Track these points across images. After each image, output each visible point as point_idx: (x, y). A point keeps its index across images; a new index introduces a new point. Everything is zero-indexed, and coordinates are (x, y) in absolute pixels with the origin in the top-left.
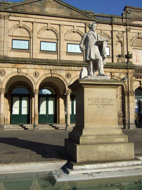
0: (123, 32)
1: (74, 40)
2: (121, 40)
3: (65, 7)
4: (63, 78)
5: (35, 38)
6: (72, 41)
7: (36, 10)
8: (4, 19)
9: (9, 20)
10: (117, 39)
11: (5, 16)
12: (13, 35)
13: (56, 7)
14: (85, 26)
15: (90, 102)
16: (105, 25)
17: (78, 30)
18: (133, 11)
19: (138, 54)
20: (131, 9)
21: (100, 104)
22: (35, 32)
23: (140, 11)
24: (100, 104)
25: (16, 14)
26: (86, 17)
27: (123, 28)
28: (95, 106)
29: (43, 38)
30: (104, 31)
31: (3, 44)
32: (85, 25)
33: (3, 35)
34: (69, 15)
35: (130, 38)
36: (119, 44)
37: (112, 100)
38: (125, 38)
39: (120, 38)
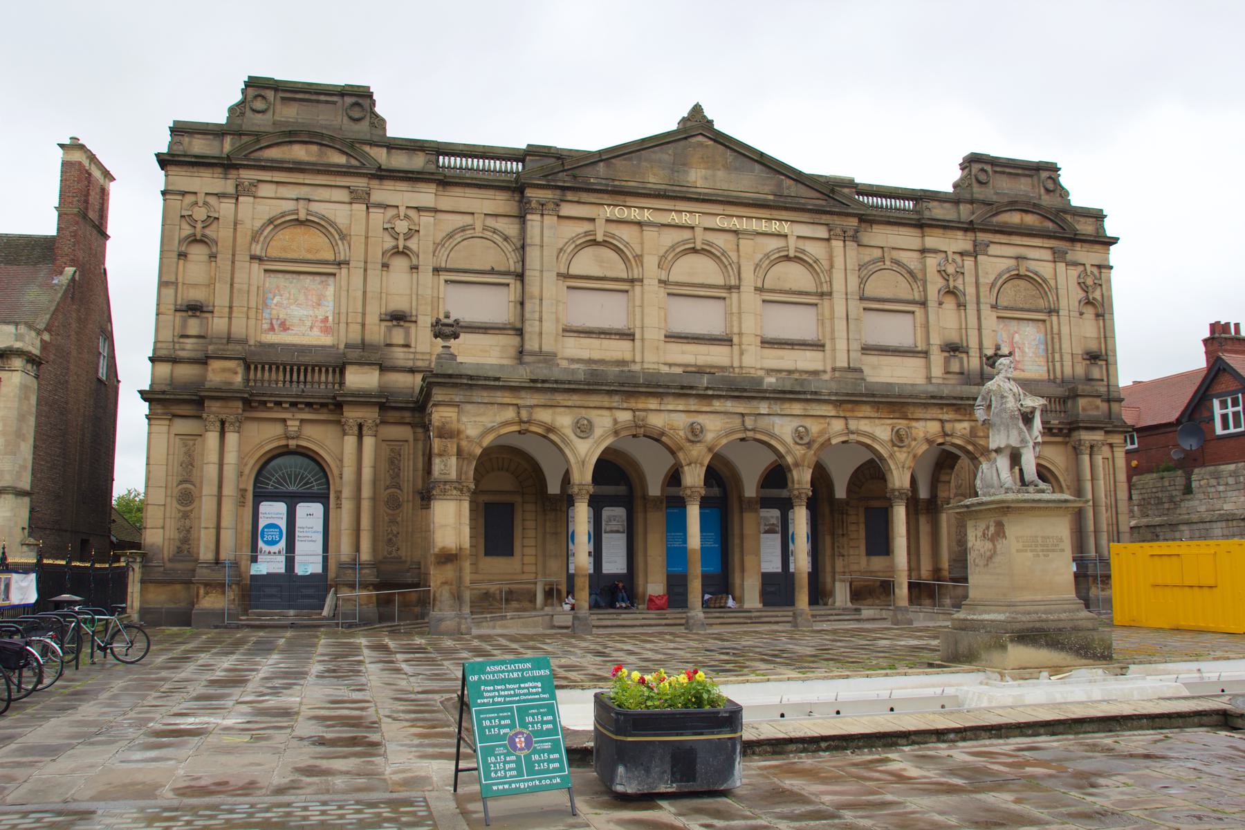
0: (962, 254)
1: (787, 286)
2: (955, 287)
3: (757, 166)
4: (784, 443)
5: (651, 284)
6: (781, 292)
7: (655, 179)
8: (542, 215)
9: (559, 217)
10: (940, 283)
11: (543, 201)
12: (573, 271)
13: (727, 167)
14: (826, 235)
15: (1020, 546)
16: (895, 228)
17: (803, 252)
18: (996, 172)
19: (1017, 337)
20: (988, 168)
21: (1039, 548)
22: (651, 262)
23: (1020, 171)
24: (1039, 548)
25: (585, 197)
26: (832, 202)
27: (961, 242)
28: (1030, 554)
29: (677, 284)
30: (896, 255)
31: (537, 308)
32: (830, 231)
33: (537, 274)
34: (771, 197)
35: (986, 280)
36: (950, 303)
37: (1061, 540)
38: (970, 279)
39: (951, 279)
